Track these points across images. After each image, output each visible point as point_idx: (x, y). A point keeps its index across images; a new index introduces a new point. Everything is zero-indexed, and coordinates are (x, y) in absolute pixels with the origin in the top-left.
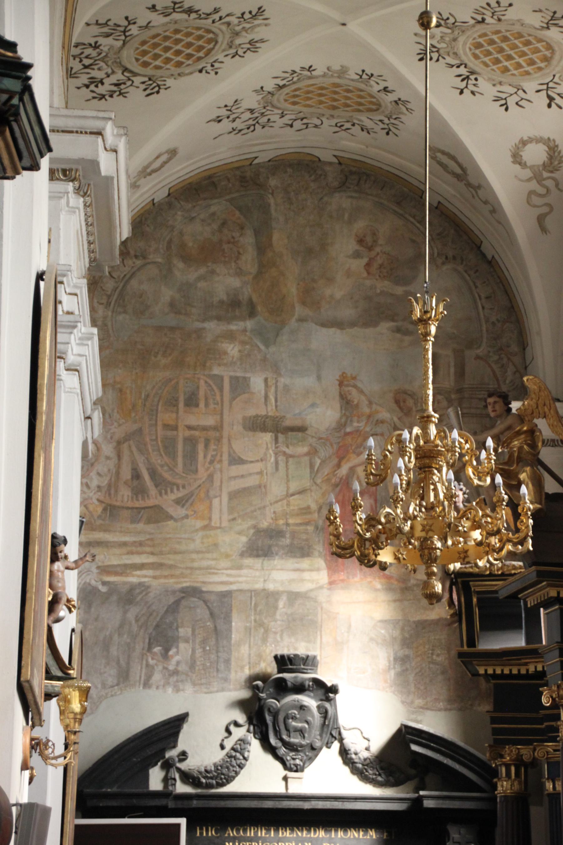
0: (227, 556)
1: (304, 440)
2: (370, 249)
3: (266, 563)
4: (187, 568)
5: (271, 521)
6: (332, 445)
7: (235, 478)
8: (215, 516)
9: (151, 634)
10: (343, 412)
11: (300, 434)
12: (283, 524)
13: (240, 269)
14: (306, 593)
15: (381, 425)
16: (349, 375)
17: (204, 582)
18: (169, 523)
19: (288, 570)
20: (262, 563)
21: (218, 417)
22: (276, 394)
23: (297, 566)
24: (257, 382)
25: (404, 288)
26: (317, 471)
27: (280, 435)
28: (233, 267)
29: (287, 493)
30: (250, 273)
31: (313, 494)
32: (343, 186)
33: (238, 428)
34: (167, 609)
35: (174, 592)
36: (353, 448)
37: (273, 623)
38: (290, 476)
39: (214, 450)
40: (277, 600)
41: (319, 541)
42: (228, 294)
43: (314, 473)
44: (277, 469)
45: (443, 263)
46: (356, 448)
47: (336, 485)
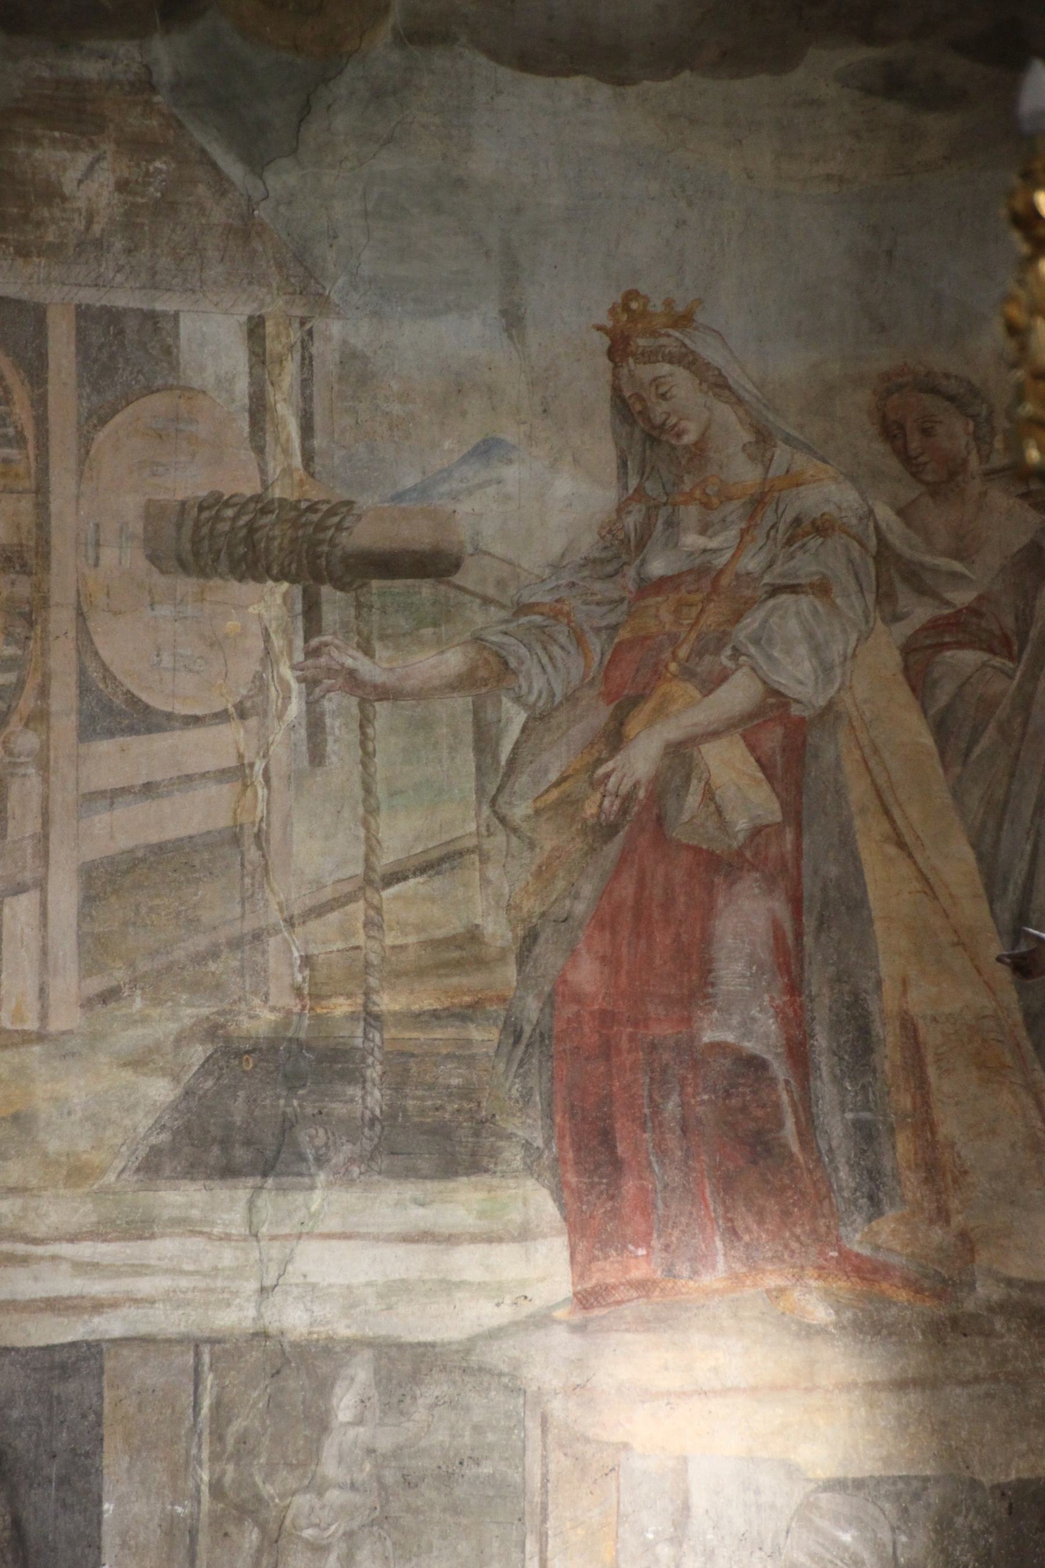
0: (78, 1173)
3: (266, 1202)
7: (112, 796)
11: (426, 589)
14: (469, 1346)
15: (814, 543)
16: (657, 305)
19: (376, 1238)
21: (26, 504)
22: (307, 399)
26: (512, 761)
29: (369, 867)
33: (123, 558)
36: (683, 652)
37: (303, 1501)
40: (324, 1387)
41: (526, 1096)
43: (495, 777)
44: (317, 756)
46: (699, 653)
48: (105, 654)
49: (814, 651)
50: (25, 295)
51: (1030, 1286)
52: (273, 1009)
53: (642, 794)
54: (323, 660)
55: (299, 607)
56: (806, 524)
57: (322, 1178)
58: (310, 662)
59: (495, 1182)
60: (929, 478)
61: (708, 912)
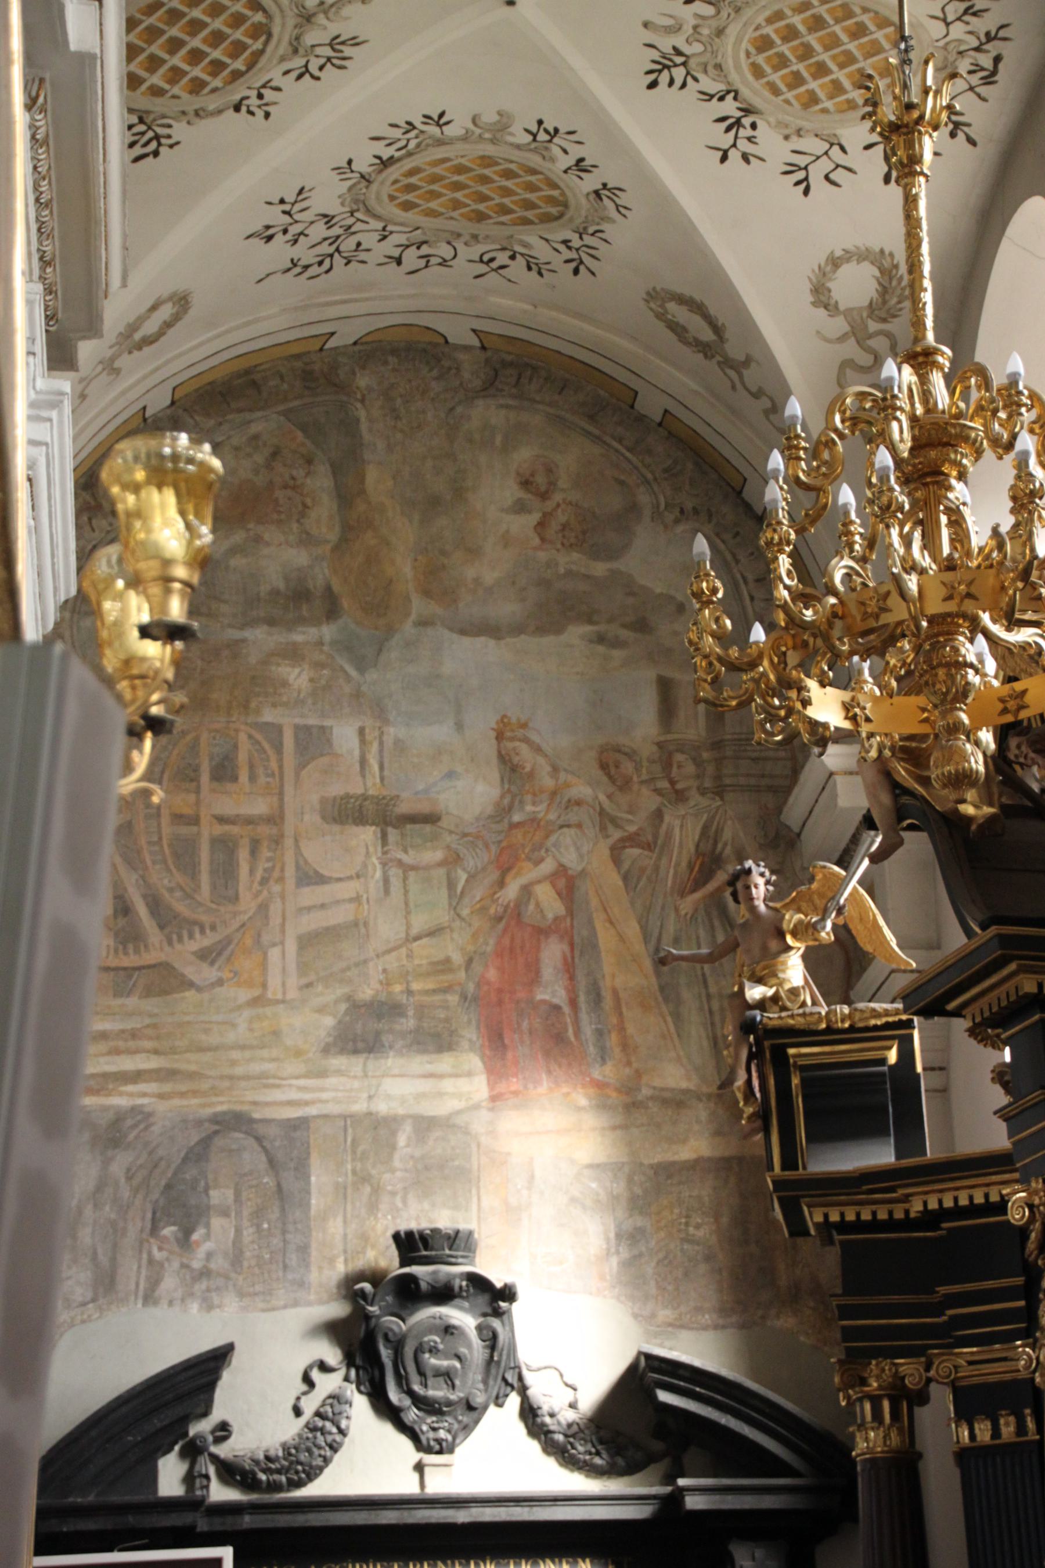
0: (298, 1053)
1: (435, 837)
2: (544, 496)
3: (371, 1064)
4: (222, 1077)
5: (378, 986)
6: (487, 846)
7: (309, 909)
8: (274, 981)
9: (157, 1201)
10: (506, 786)
11: (428, 828)
12: (402, 992)
13: (308, 534)
15: (576, 808)
16: (514, 720)
17: (255, 1103)
18: (187, 994)
19: (413, 1076)
20: (365, 1065)
21: (275, 799)
22: (381, 757)
23: (429, 1068)
24: (345, 735)
25: (609, 565)
26: (462, 893)
27: (390, 830)
28: (295, 530)
29: (407, 934)
30: (327, 542)
31: (455, 936)
32: (489, 387)
33: (312, 818)
34: (187, 1154)
35: (199, 1123)
37: (387, 1176)
38: (412, 905)
39: (269, 860)
40: (394, 1133)
41: (469, 1022)
42: (286, 579)
43: (456, 898)
44: (387, 891)
45: (677, 521)
46: (533, 850)
47: (499, 919)
48: (306, 855)
49: (577, 850)
51: (662, 1089)
61: (538, 950)
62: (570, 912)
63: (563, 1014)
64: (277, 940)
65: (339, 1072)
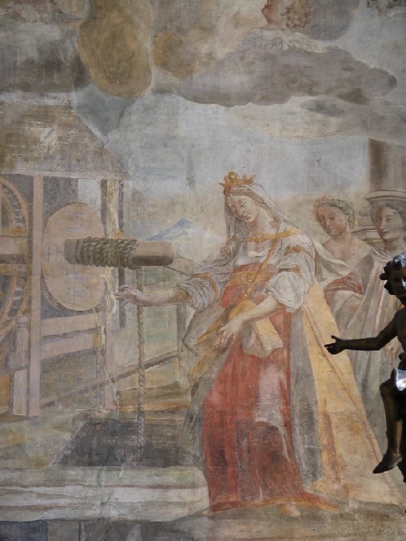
0: (39, 464)
1: (167, 277)
5: (114, 408)
6: (213, 286)
7: (52, 337)
8: (19, 400)
11: (161, 269)
12: (134, 412)
13: (60, 12)
15: (294, 255)
16: (240, 177)
19: (142, 487)
20: (99, 476)
21: (25, 241)
22: (121, 206)
23: (157, 480)
24: (89, 188)
25: (328, 44)
26: (190, 327)
27: (126, 269)
28: (49, 9)
29: (140, 362)
30: (78, 19)
31: (183, 364)
33: (57, 259)
38: (144, 336)
39: (18, 293)
41: (194, 439)
42: (40, 51)
43: (184, 332)
44: (122, 324)
47: (224, 350)
50: (26, 174)
51: (368, 504)
52: (107, 409)
53: (235, 338)
54: (125, 293)
55: (117, 275)
56: (291, 249)
57: (122, 468)
58: (121, 293)
59: (183, 468)
60: (333, 233)
61: (257, 378)
62: (288, 346)
63: (279, 435)
64: (23, 364)
65: (75, 482)
